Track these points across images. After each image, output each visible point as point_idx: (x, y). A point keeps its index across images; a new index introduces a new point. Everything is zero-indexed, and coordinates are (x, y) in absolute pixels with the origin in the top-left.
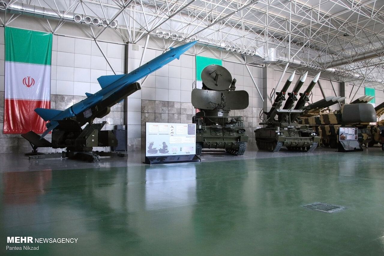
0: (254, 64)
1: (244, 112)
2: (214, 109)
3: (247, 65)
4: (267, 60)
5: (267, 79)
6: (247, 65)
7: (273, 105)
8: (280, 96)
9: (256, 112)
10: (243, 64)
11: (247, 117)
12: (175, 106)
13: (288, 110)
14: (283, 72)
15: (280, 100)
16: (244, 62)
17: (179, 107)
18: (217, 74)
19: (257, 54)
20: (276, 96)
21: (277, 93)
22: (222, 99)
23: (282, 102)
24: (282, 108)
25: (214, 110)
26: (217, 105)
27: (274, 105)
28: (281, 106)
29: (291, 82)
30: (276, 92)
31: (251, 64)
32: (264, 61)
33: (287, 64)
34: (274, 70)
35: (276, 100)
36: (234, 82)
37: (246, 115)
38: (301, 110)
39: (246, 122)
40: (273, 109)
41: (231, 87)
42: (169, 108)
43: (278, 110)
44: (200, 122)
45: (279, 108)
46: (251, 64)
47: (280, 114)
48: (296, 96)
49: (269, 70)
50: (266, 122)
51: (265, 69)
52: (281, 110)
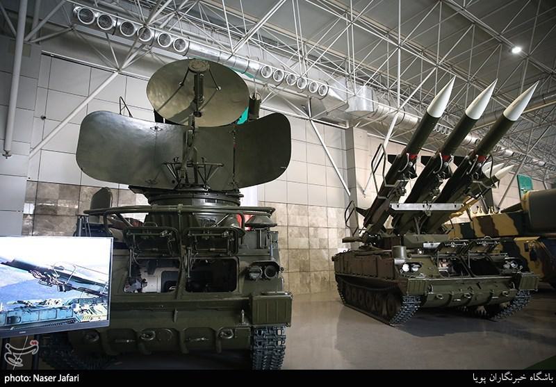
0: (325, 120)
1: (310, 218)
2: (176, 187)
4: (352, 108)
9: (335, 217)
10: (304, 119)
11: (316, 228)
12: (137, 199)
13: (422, 205)
14: (384, 140)
15: (399, 176)
18: (197, 74)
19: (332, 93)
20: (389, 165)
21: (391, 158)
23: (405, 183)
24: (403, 199)
30: (388, 155)
32: (347, 111)
33: (392, 121)
34: (369, 136)
35: (390, 178)
36: (254, 105)
37: (314, 222)
38: (457, 205)
39: (315, 237)
40: (378, 203)
43: (394, 206)
45: (396, 199)
47: (398, 215)
48: (447, 164)
49: (359, 135)
51: (349, 133)
52: (402, 205)
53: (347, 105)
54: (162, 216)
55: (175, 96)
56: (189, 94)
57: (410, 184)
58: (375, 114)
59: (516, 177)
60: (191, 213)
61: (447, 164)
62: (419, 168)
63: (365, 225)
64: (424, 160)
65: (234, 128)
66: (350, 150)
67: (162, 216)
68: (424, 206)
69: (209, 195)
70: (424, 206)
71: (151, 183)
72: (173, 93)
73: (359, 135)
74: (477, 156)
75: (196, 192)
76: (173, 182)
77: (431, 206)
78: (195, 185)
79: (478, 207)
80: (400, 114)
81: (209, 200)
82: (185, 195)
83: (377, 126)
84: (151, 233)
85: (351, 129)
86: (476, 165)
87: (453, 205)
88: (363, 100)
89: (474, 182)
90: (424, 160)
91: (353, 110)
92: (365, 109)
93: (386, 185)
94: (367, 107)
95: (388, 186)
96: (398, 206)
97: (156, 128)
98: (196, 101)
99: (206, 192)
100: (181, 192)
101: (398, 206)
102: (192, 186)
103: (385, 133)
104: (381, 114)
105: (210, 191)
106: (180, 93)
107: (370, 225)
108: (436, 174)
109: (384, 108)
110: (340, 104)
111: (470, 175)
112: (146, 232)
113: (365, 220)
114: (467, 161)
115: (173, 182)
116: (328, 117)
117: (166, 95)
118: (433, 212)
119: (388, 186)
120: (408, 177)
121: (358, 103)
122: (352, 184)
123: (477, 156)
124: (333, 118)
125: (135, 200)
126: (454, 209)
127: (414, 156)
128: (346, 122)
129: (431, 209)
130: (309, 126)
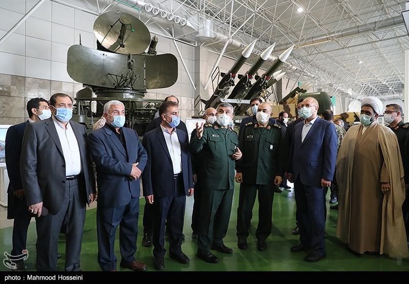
0: (183, 40)
2: (116, 87)
4: (201, 34)
5: (200, 61)
8: (226, 79)
9: (185, 103)
12: (63, 88)
13: (236, 100)
15: (226, 85)
18: (123, 25)
20: (221, 78)
21: (222, 74)
23: (229, 89)
24: (227, 96)
25: (115, 89)
26: (119, 78)
27: (217, 92)
29: (246, 58)
32: (197, 36)
33: (225, 44)
35: (221, 85)
36: (153, 44)
40: (213, 98)
41: (149, 52)
43: (222, 100)
44: (81, 109)
45: (223, 96)
48: (250, 80)
49: (203, 50)
50: (203, 115)
51: (198, 49)
53: (198, 33)
56: (116, 33)
57: (232, 88)
58: (214, 39)
59: (297, 83)
60: (134, 102)
61: (250, 80)
62: (237, 80)
64: (240, 76)
66: (197, 61)
69: (132, 92)
71: (103, 84)
73: (203, 50)
75: (125, 90)
76: (114, 84)
78: (127, 86)
80: (231, 40)
81: (132, 94)
82: (119, 91)
83: (215, 45)
85: (198, 47)
88: (207, 29)
90: (240, 76)
91: (201, 36)
92: (208, 36)
93: (219, 89)
94: (210, 35)
98: (121, 37)
102: (125, 87)
104: (218, 40)
105: (133, 90)
106: (112, 32)
109: (219, 35)
114: (261, 79)
116: (185, 38)
117: (104, 33)
118: (242, 104)
120: (230, 86)
121: (205, 31)
122: (197, 82)
124: (188, 39)
128: (195, 42)
129: (241, 103)
130: (172, 44)
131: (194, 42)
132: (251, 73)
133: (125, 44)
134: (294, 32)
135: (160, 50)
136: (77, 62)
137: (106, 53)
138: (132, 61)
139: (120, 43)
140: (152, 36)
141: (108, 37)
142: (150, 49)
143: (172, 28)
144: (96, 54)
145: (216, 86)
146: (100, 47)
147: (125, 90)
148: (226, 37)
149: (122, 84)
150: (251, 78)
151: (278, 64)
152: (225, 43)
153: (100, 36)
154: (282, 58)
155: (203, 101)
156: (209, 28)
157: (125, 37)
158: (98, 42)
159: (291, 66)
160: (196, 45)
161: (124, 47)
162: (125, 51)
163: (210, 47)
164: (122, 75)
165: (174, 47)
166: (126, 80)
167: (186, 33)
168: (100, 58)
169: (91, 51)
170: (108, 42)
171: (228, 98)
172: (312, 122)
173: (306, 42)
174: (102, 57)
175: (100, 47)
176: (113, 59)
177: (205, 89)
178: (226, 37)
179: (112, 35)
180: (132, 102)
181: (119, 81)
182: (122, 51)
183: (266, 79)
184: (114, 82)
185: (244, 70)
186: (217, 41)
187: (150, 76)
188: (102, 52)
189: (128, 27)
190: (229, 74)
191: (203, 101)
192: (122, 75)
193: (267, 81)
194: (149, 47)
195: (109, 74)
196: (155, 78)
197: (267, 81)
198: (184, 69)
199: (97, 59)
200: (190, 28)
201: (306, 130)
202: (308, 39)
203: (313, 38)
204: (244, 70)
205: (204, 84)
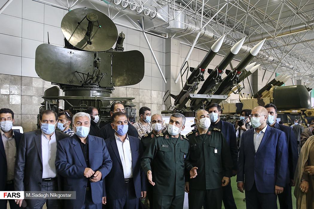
0: (154, 33)
1: (140, 97)
2: (83, 85)
3: (146, 33)
4: (172, 26)
6: (144, 33)
7: (184, 88)
8: (195, 74)
9: (156, 97)
13: (206, 95)
15: (195, 80)
16: (139, 28)
17: (41, 86)
20: (190, 73)
21: (192, 69)
22: (95, 64)
23: (198, 84)
25: (82, 86)
26: (86, 76)
27: (186, 87)
28: (196, 89)
31: (151, 31)
32: (168, 28)
35: (190, 80)
36: (120, 40)
37: (143, 99)
38: (225, 96)
40: (182, 93)
41: (116, 49)
42: (23, 87)
43: (191, 95)
44: (48, 107)
45: (193, 91)
46: (151, 31)
47: (194, 100)
48: (220, 75)
49: (175, 42)
51: (168, 41)
52: (196, 95)
53: (168, 25)
54: (87, 101)
55: (76, 31)
56: (83, 30)
57: (201, 83)
58: (185, 30)
59: (274, 74)
60: (100, 100)
61: (220, 75)
62: (206, 75)
63: (175, 105)
64: (210, 71)
65: (109, 52)
66: (168, 53)
67: (83, 101)
68: (207, 96)
69: (99, 89)
70: (207, 96)
71: (70, 82)
72: (74, 30)
73: (175, 42)
74: (237, 71)
76: (81, 82)
77: (211, 96)
79: (248, 95)
80: (203, 31)
81: (98, 91)
83: (186, 36)
84: (83, 109)
86: (236, 75)
87: (223, 96)
88: (179, 20)
89: (234, 85)
90: (210, 71)
92: (179, 27)
93: (188, 85)
94: (181, 26)
95: (189, 85)
96: (193, 95)
97: (71, 52)
98: (88, 34)
99: (97, 87)
100: (85, 87)
101: (193, 95)
102: (92, 84)
103: (192, 42)
104: (190, 31)
105: (100, 87)
106: (79, 29)
107: (178, 105)
108: (215, 80)
109: (192, 27)
110: (164, 24)
111: (232, 81)
112: (81, 109)
113: (175, 102)
114: (231, 73)
115: (81, 82)
117: (71, 30)
118: (212, 100)
119: (189, 85)
120: (200, 81)
121: (175, 24)
122: (168, 76)
123: (237, 71)
124: (159, 31)
125: (32, 84)
126: (223, 98)
127: (204, 70)
128: (165, 34)
129: (211, 98)
130: (142, 36)
131: (165, 34)
132: (221, 67)
133: (92, 40)
134: (271, 21)
135: (127, 47)
136: (45, 61)
137: (73, 51)
138: (98, 59)
139: (87, 40)
140: (119, 33)
141: (75, 35)
142: (117, 46)
143: (142, 20)
144: (63, 52)
145: (185, 81)
146: (68, 45)
147: (92, 87)
148: (198, 28)
149: (89, 81)
150: (221, 72)
151: (249, 58)
152: (197, 34)
153: (67, 35)
154: (254, 51)
155: (173, 96)
156: (180, 20)
157: (93, 33)
158: (65, 39)
159: (267, 56)
160: (167, 37)
161: (91, 44)
162: (92, 48)
163: (182, 38)
164: (88, 73)
165: (145, 40)
166: (92, 78)
167: (156, 24)
168: (68, 57)
169: (59, 49)
170: (75, 40)
171: (198, 93)
172: (264, 130)
173: (283, 31)
174: (69, 55)
175: (68, 45)
176: (80, 56)
177: (176, 82)
178: (198, 29)
179: (79, 32)
180: (98, 100)
181: (86, 80)
182: (89, 48)
183: (238, 73)
184: (82, 80)
185: (213, 65)
186: (188, 32)
187: (117, 73)
188: (70, 50)
189: (95, 24)
190: (198, 69)
191: (173, 96)
192: (88, 73)
193: (238, 76)
194: (116, 42)
195: (76, 72)
196: (121, 75)
197: (238, 76)
198: (154, 62)
199: (65, 57)
200: (161, 20)
201: (258, 139)
202: (285, 28)
203: (290, 27)
204: (213, 65)
205: (175, 78)
